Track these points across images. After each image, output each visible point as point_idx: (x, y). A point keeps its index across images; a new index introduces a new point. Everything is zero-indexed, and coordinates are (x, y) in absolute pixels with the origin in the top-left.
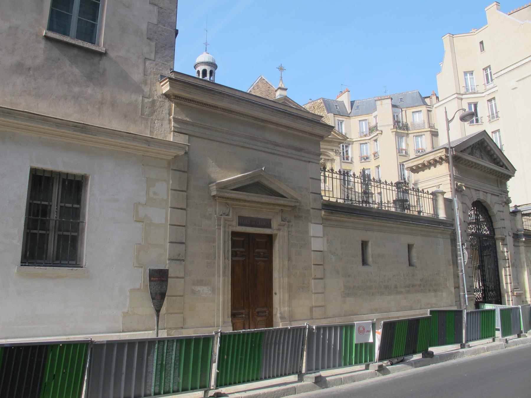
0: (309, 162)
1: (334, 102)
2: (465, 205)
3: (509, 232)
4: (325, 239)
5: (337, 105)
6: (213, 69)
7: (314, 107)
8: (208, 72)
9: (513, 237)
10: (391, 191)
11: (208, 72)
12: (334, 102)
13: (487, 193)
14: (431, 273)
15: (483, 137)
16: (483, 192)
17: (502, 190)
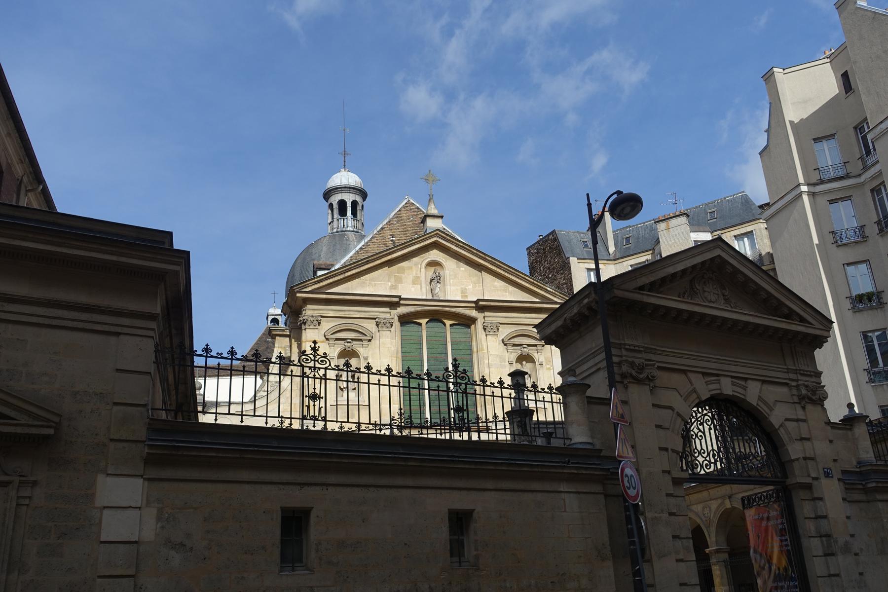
0: (118, 334)
1: (580, 236)
2: (670, 411)
3: (824, 469)
4: (151, 514)
5: (586, 240)
6: (358, 199)
7: (543, 249)
8: (349, 205)
9: (839, 480)
10: (384, 389)
11: (349, 205)
12: (580, 236)
13: (746, 379)
14: (533, 582)
15: (717, 252)
16: (732, 377)
17: (796, 370)
